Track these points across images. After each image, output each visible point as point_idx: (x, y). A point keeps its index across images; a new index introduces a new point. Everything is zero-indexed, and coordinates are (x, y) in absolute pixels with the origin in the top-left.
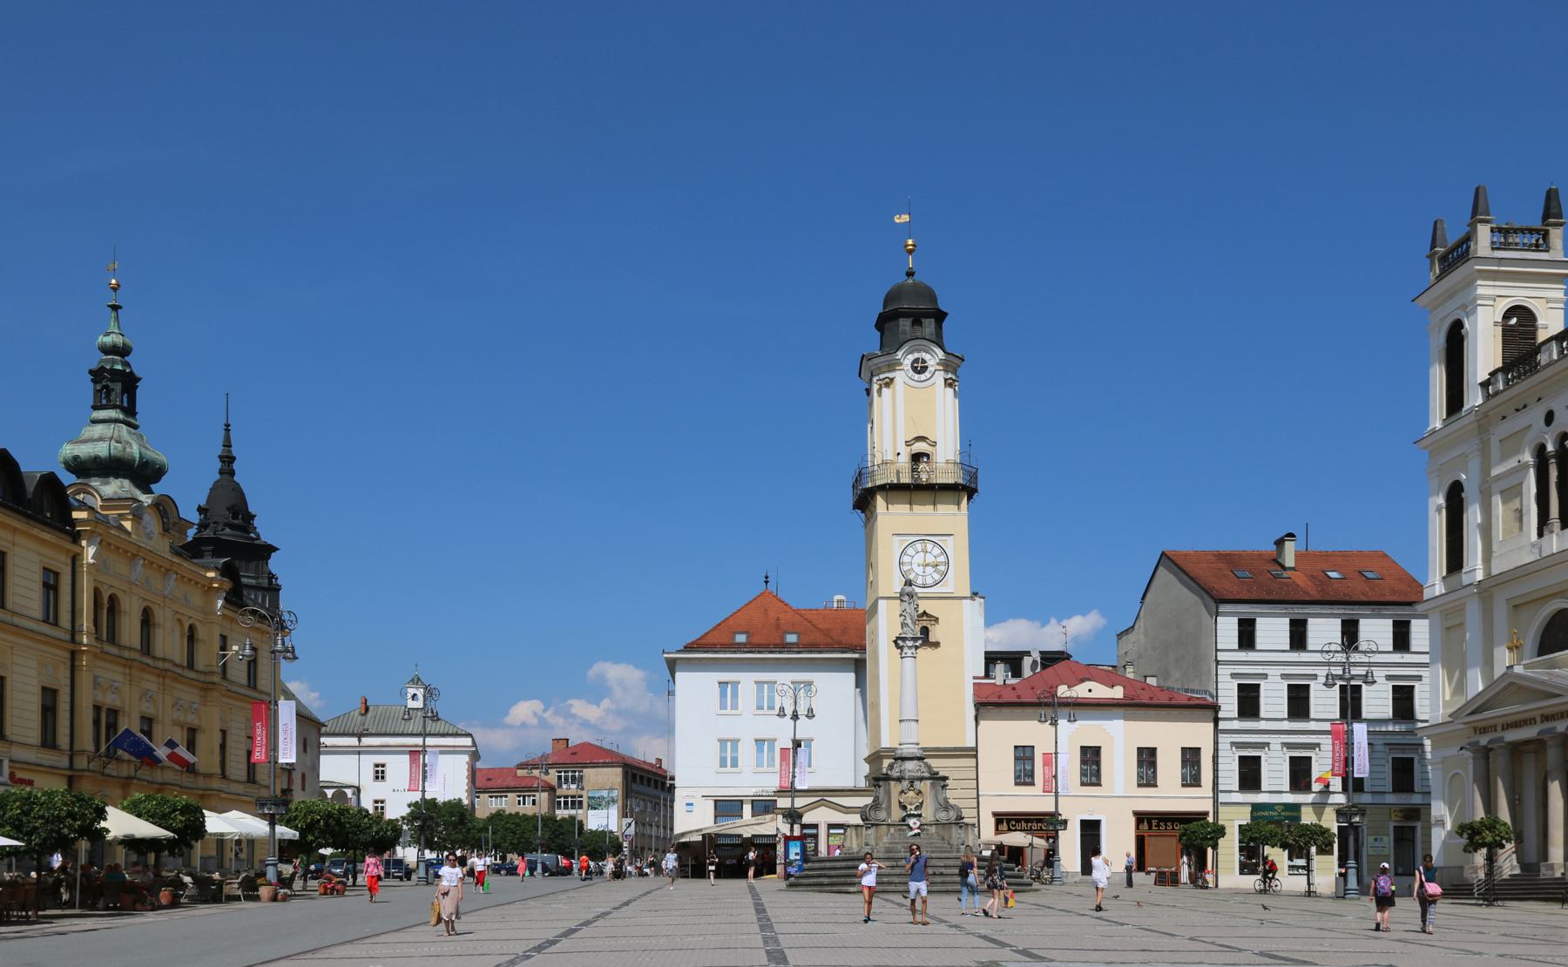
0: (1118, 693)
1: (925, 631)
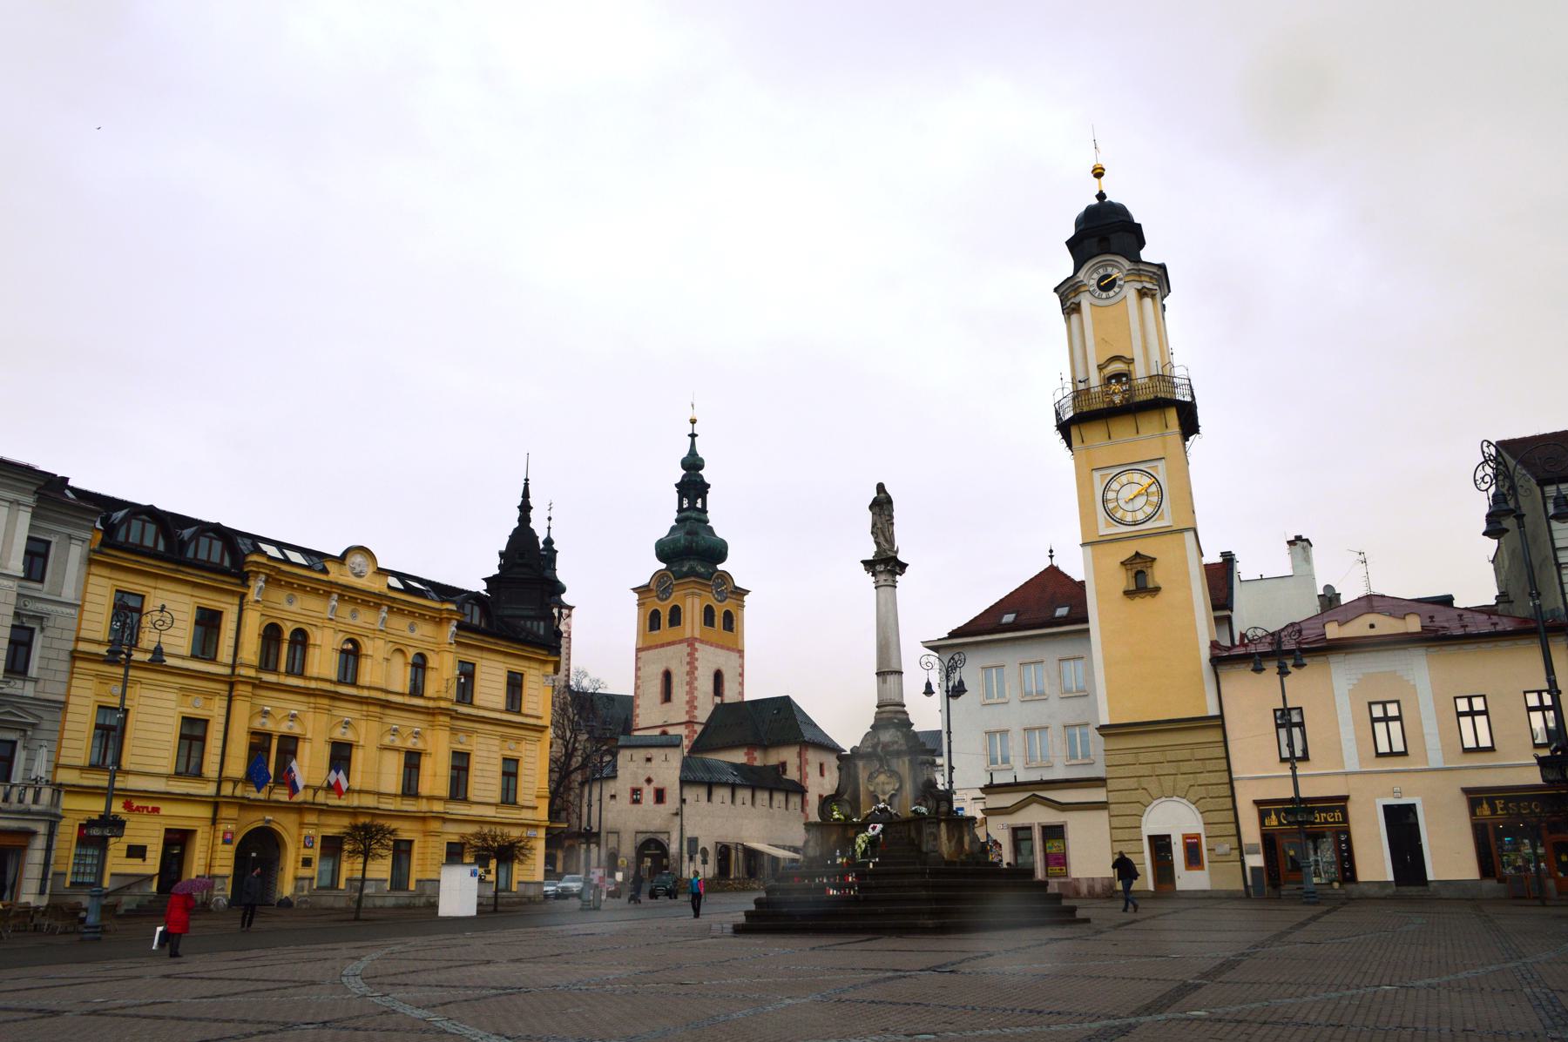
1: (1140, 575)
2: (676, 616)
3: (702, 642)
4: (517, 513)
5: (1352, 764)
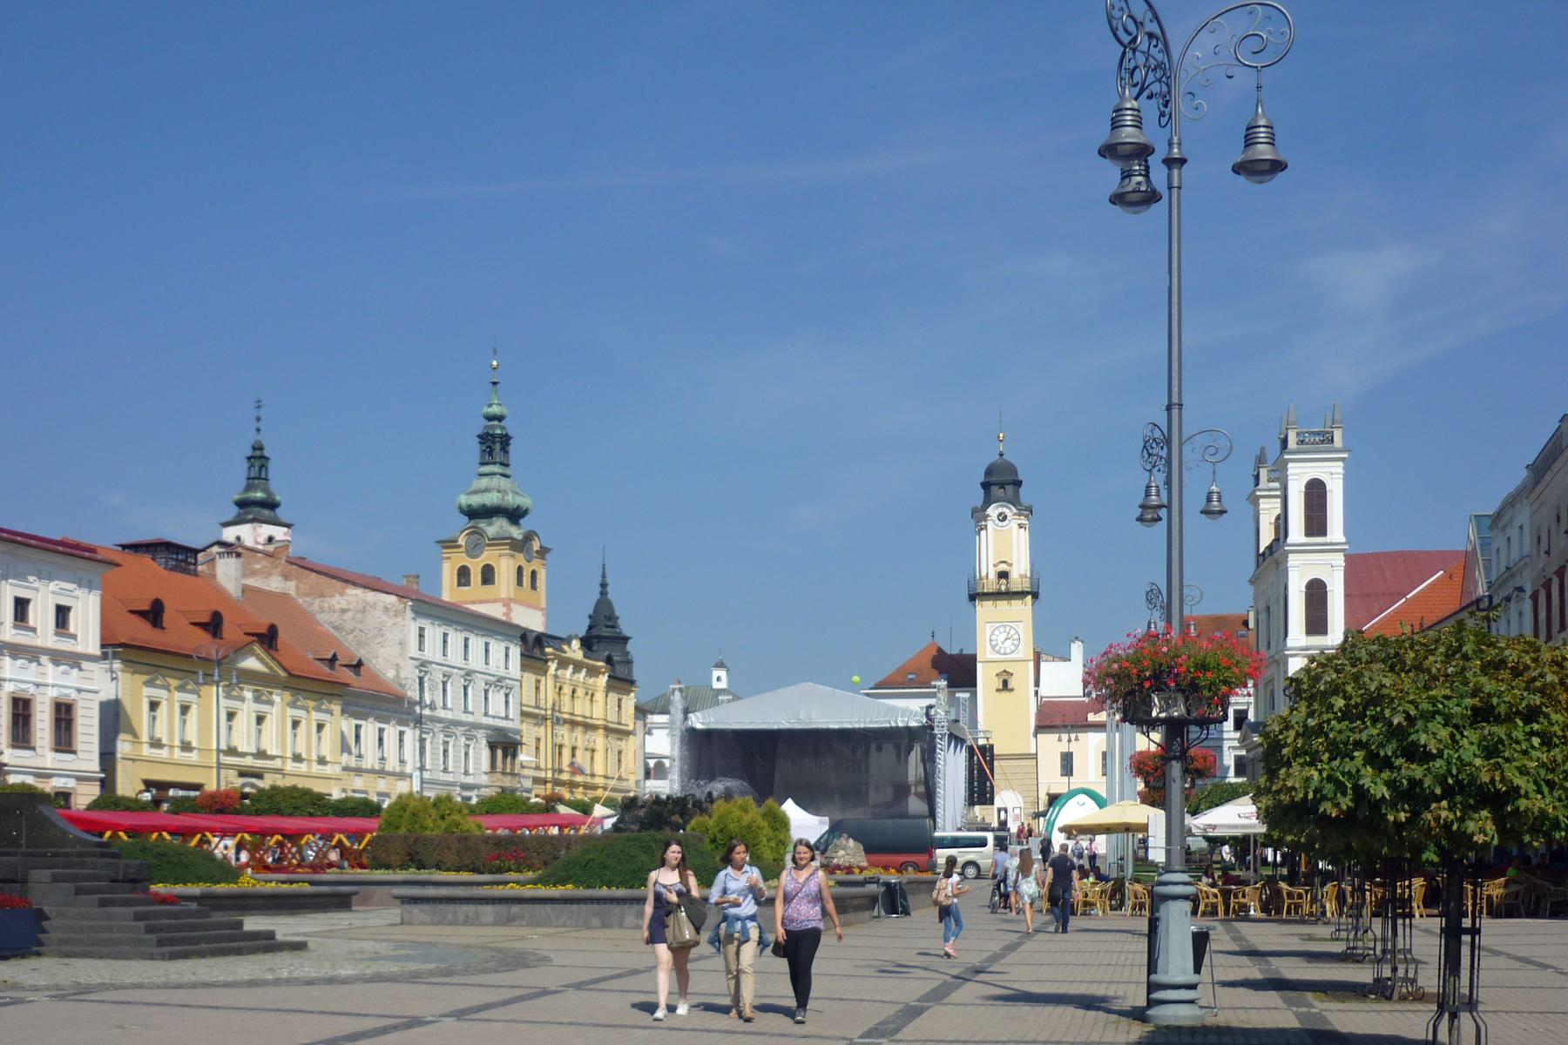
1: (1005, 683)
2: (488, 575)
3: (516, 602)
4: (599, 589)
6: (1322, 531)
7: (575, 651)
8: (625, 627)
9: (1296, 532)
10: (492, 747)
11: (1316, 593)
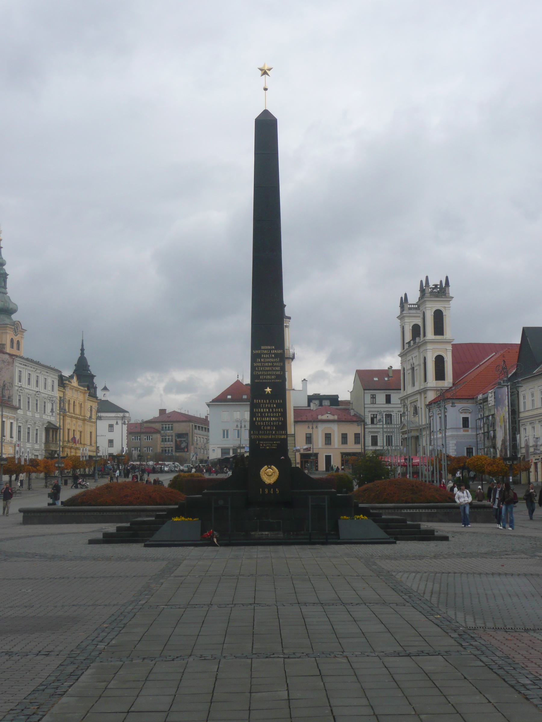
0: (336, 417)
4: (80, 352)
5: (320, 446)
6: (442, 334)
7: (75, 382)
8: (93, 370)
9: (430, 334)
10: (47, 430)
11: (440, 361)
